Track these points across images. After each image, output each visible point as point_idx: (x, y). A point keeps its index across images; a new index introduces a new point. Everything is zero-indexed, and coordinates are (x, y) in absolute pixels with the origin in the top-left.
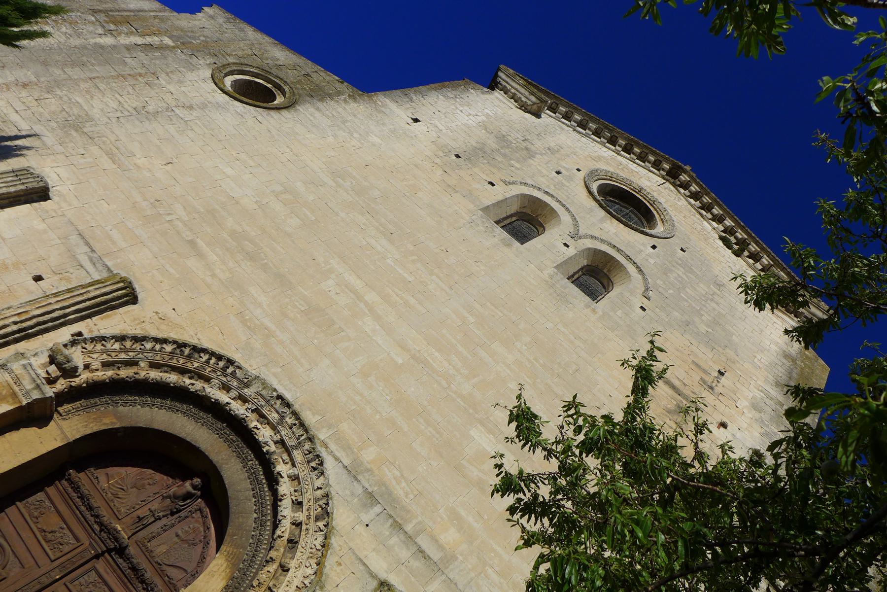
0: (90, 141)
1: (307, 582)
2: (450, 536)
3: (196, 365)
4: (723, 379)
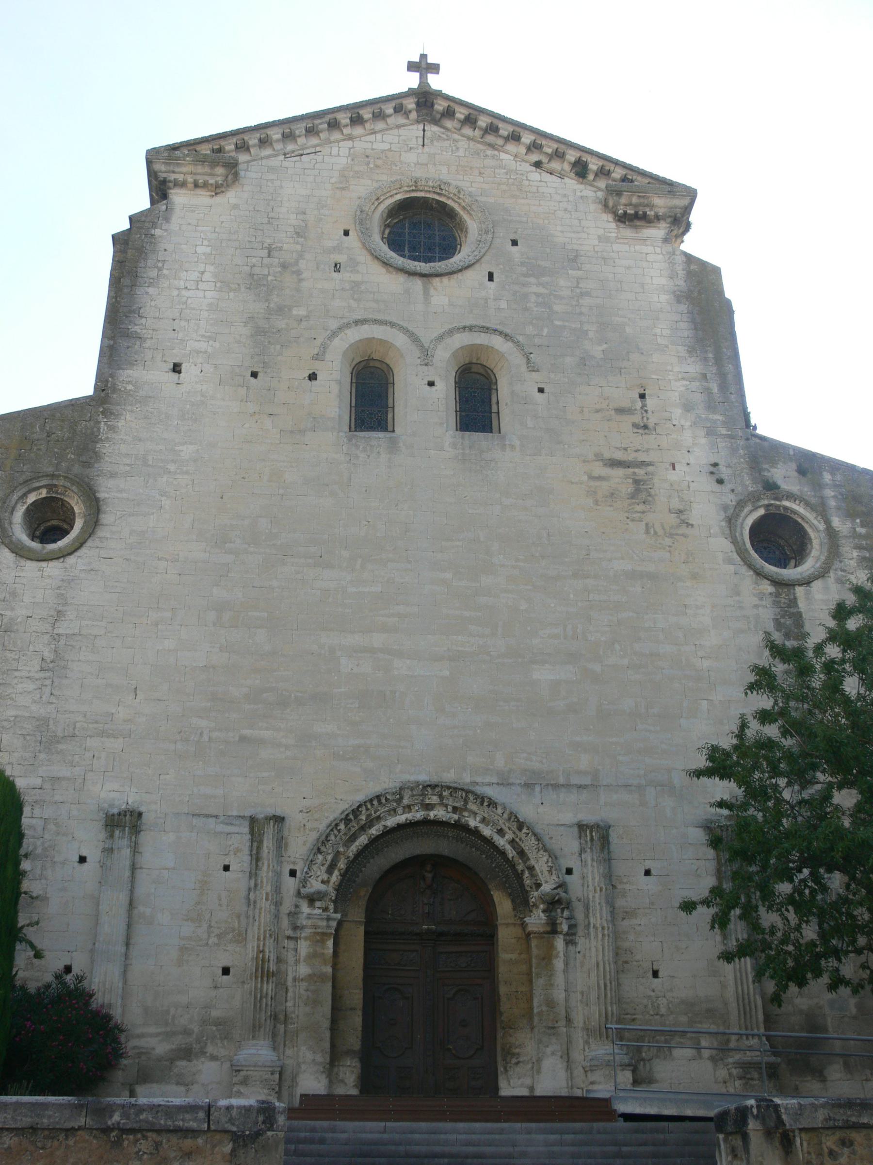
0: (77, 739)
1: (550, 864)
2: (584, 762)
3: (364, 818)
4: (649, 401)
